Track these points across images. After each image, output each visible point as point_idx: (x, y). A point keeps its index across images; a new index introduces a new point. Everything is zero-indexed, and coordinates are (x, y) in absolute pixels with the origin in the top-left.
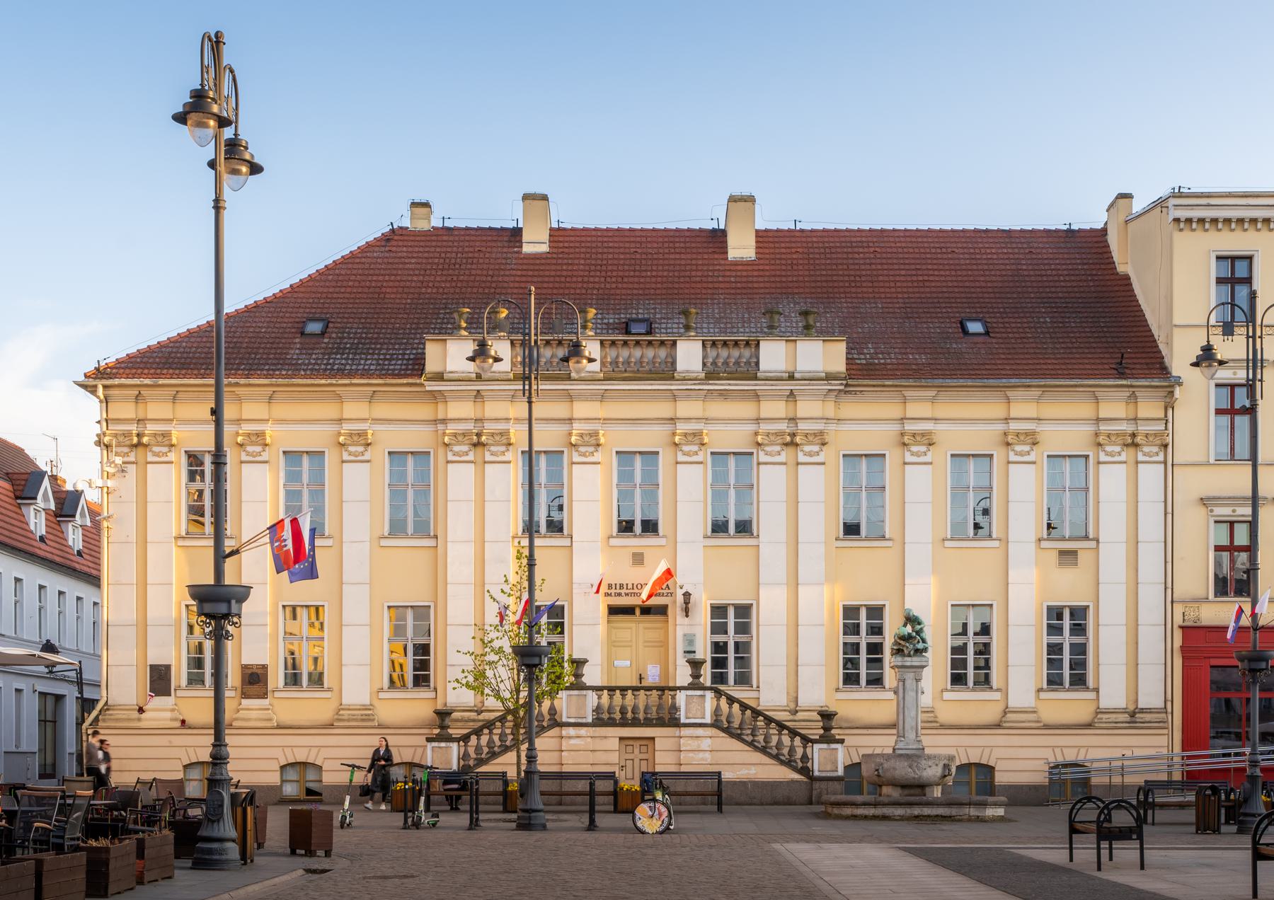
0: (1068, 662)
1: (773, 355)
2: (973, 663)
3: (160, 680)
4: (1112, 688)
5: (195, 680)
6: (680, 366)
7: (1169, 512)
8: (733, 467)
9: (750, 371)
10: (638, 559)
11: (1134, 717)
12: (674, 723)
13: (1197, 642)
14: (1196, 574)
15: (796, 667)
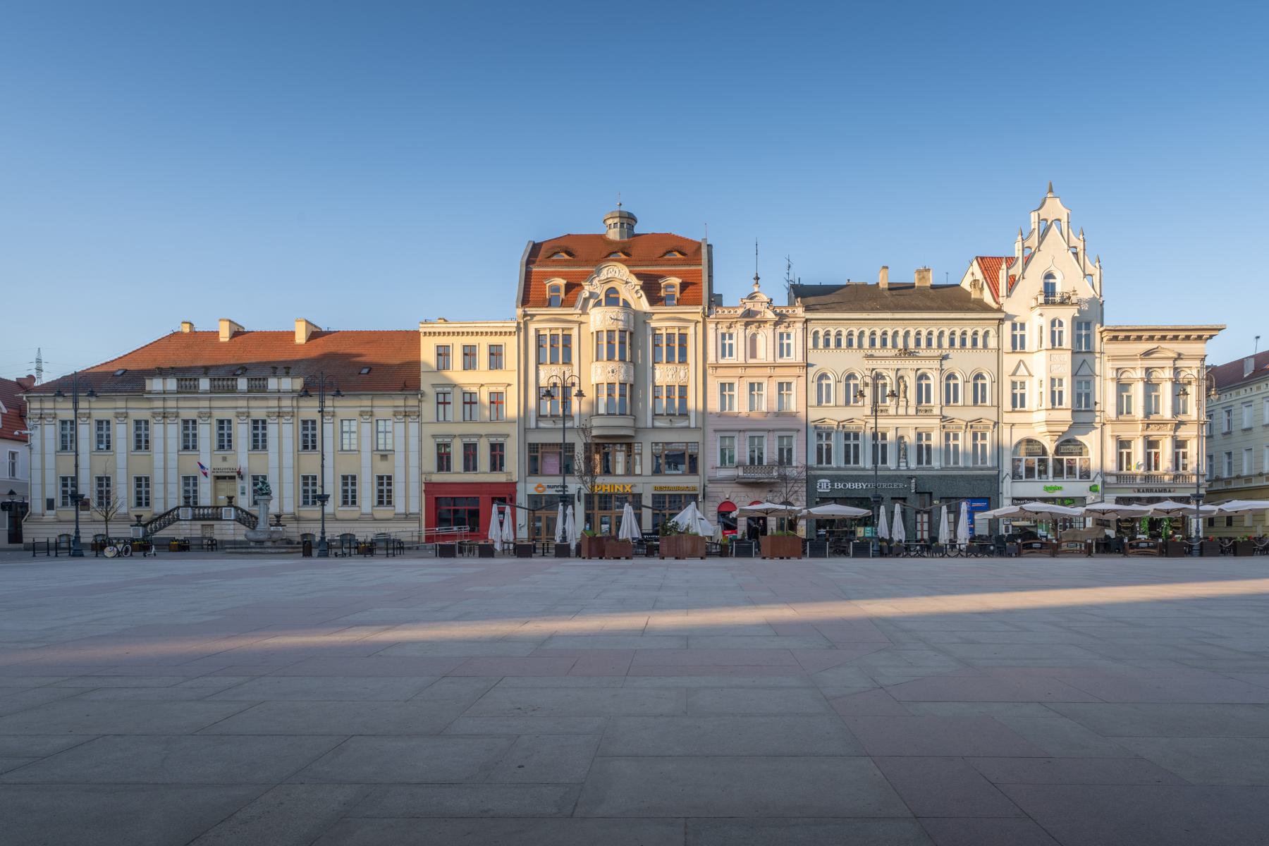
0: (384, 496)
1: (273, 384)
2: (349, 498)
3: (50, 504)
4: (400, 507)
5: (100, 504)
6: (239, 387)
7: (420, 441)
8: (258, 426)
9: (263, 389)
10: (224, 459)
11: (407, 517)
12: (221, 519)
13: (430, 488)
14: (431, 463)
15: (285, 499)
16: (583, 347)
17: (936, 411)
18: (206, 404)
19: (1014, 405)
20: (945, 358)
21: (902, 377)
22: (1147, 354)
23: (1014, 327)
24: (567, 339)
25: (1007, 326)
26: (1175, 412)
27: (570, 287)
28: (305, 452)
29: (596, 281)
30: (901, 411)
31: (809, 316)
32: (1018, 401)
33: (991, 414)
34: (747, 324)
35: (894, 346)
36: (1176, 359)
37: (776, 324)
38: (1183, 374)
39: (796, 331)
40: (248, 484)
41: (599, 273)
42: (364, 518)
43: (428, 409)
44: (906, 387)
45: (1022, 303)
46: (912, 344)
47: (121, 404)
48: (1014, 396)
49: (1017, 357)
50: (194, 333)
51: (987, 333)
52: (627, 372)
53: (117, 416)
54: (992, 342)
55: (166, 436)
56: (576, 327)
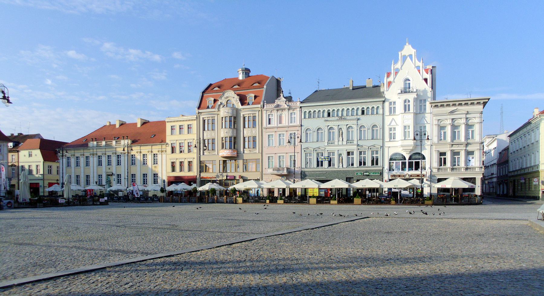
16: (218, 123)
17: (355, 142)
18: (104, 150)
19: (390, 138)
20: (358, 119)
21: (341, 129)
22: (452, 112)
23: (390, 103)
24: (213, 120)
25: (387, 104)
26: (467, 138)
27: (215, 101)
28: (133, 166)
29: (223, 98)
30: (340, 143)
31: (302, 105)
32: (392, 137)
33: (380, 143)
34: (277, 111)
35: (337, 116)
36: (466, 114)
37: (289, 110)
38: (470, 121)
39: (297, 111)
40: (115, 177)
41: (223, 94)
42: (152, 188)
43: (169, 149)
44: (342, 133)
45: (392, 94)
46: (345, 113)
47: (82, 151)
48: (390, 134)
49: (391, 117)
50: (110, 125)
51: (378, 107)
52: (233, 132)
53: (81, 155)
54: (380, 111)
55: (94, 161)
56: (216, 116)
